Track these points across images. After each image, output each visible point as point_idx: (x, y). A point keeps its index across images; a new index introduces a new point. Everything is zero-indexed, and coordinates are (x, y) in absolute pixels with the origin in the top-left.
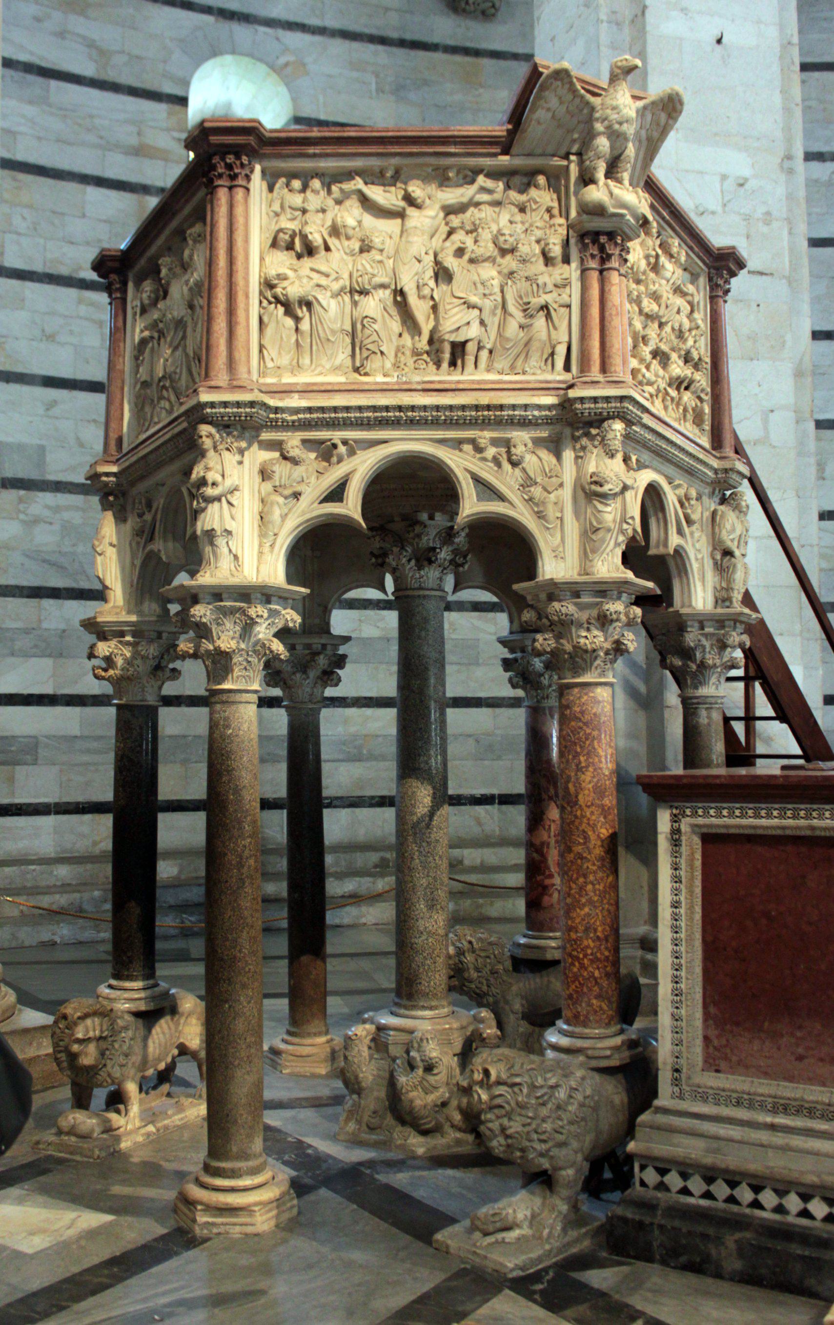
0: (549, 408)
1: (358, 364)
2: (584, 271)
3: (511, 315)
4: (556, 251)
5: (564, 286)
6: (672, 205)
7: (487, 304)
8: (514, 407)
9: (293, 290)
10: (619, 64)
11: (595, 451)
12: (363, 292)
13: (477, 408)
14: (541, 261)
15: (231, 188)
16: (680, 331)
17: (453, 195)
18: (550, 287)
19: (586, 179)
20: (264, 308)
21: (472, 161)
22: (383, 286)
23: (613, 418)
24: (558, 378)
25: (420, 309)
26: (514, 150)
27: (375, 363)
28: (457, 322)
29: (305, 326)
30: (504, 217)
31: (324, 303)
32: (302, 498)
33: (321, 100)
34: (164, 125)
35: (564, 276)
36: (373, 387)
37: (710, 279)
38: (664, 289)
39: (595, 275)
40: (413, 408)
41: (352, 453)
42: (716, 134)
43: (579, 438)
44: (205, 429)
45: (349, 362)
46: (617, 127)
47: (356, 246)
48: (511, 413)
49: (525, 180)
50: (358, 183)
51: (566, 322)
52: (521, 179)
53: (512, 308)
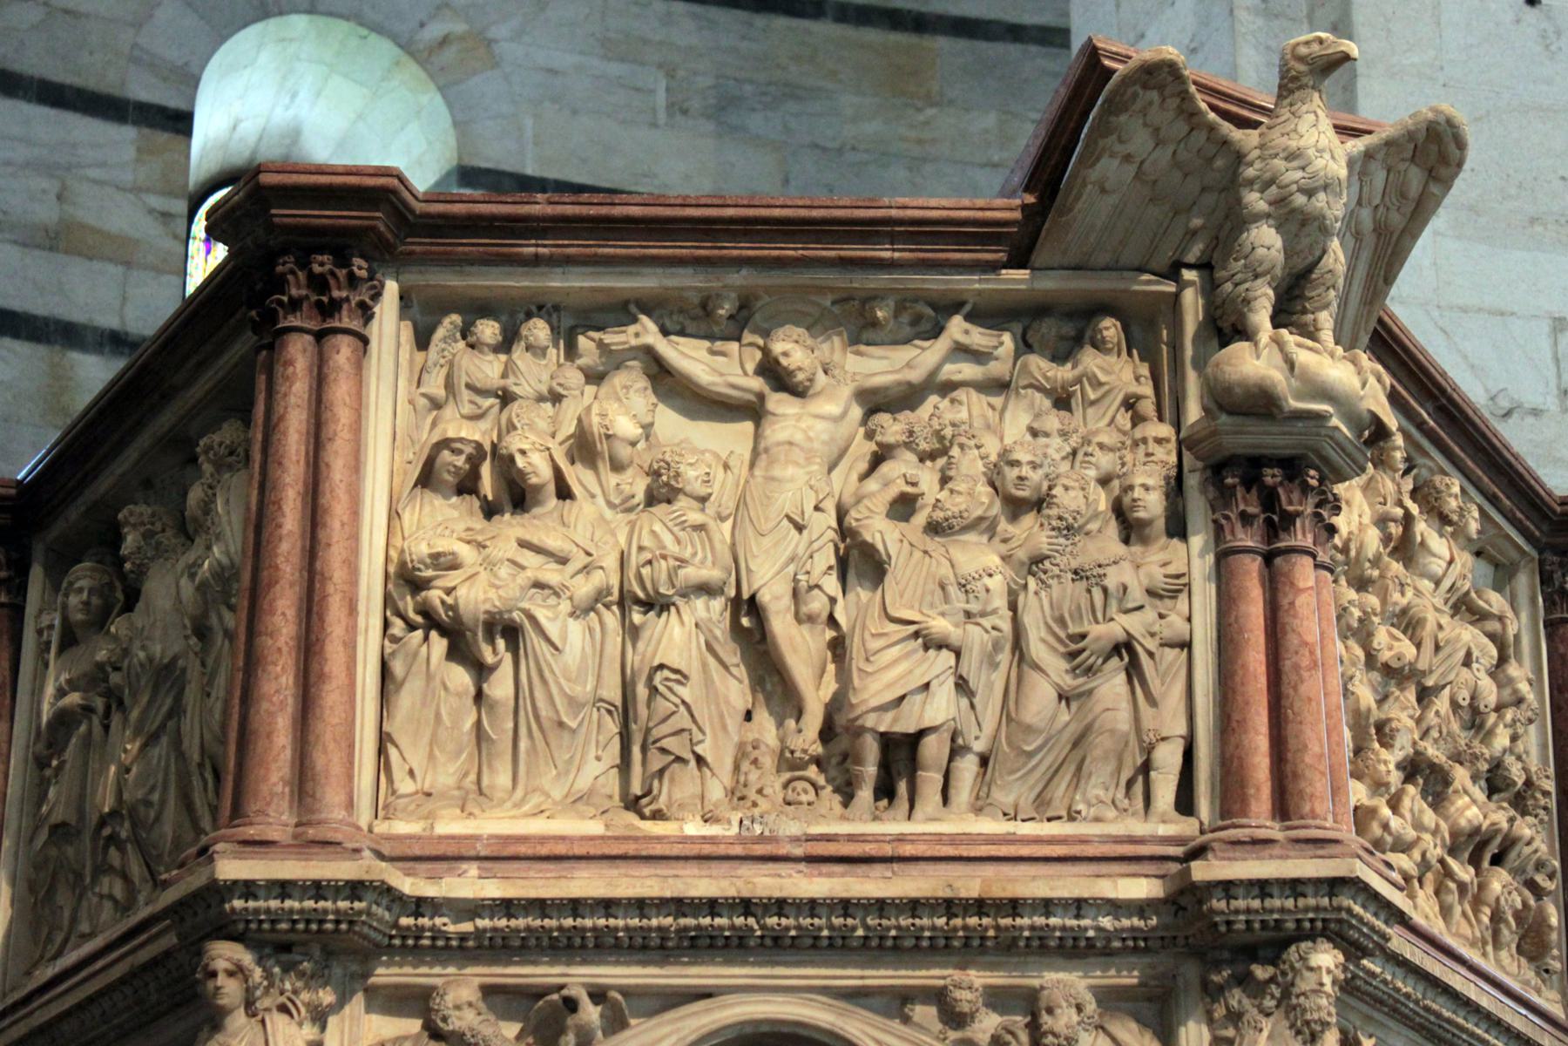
0: (1141, 908)
1: (636, 788)
2: (1224, 556)
3: (1036, 667)
4: (1152, 504)
5: (1174, 594)
6: (1443, 391)
7: (976, 638)
8: (1047, 906)
9: (474, 594)
10: (1303, 50)
11: (1267, 1025)
12: (656, 604)
13: (949, 906)
14: (1113, 529)
15: (320, 336)
16: (1474, 710)
17: (886, 365)
18: (1137, 596)
19: (1227, 327)
20: (395, 640)
21: (935, 282)
22: (706, 589)
23: (1312, 936)
24: (1163, 830)
25: (800, 649)
26: (1039, 258)
27: (681, 787)
28: (897, 683)
29: (501, 687)
30: (1017, 421)
31: (553, 630)
33: (529, 123)
34: (127, 177)
35: (1171, 570)
36: (676, 850)
37: (1546, 579)
38: (1430, 604)
39: (1252, 567)
40: (780, 906)
41: (616, 1023)
42: (1533, 221)
43: (1221, 989)
44: (225, 954)
45: (612, 783)
46: (1300, 200)
47: (639, 486)
48: (1039, 920)
49: (1068, 329)
50: (647, 332)
51: (1179, 687)
52: (1057, 326)
53: (1039, 647)
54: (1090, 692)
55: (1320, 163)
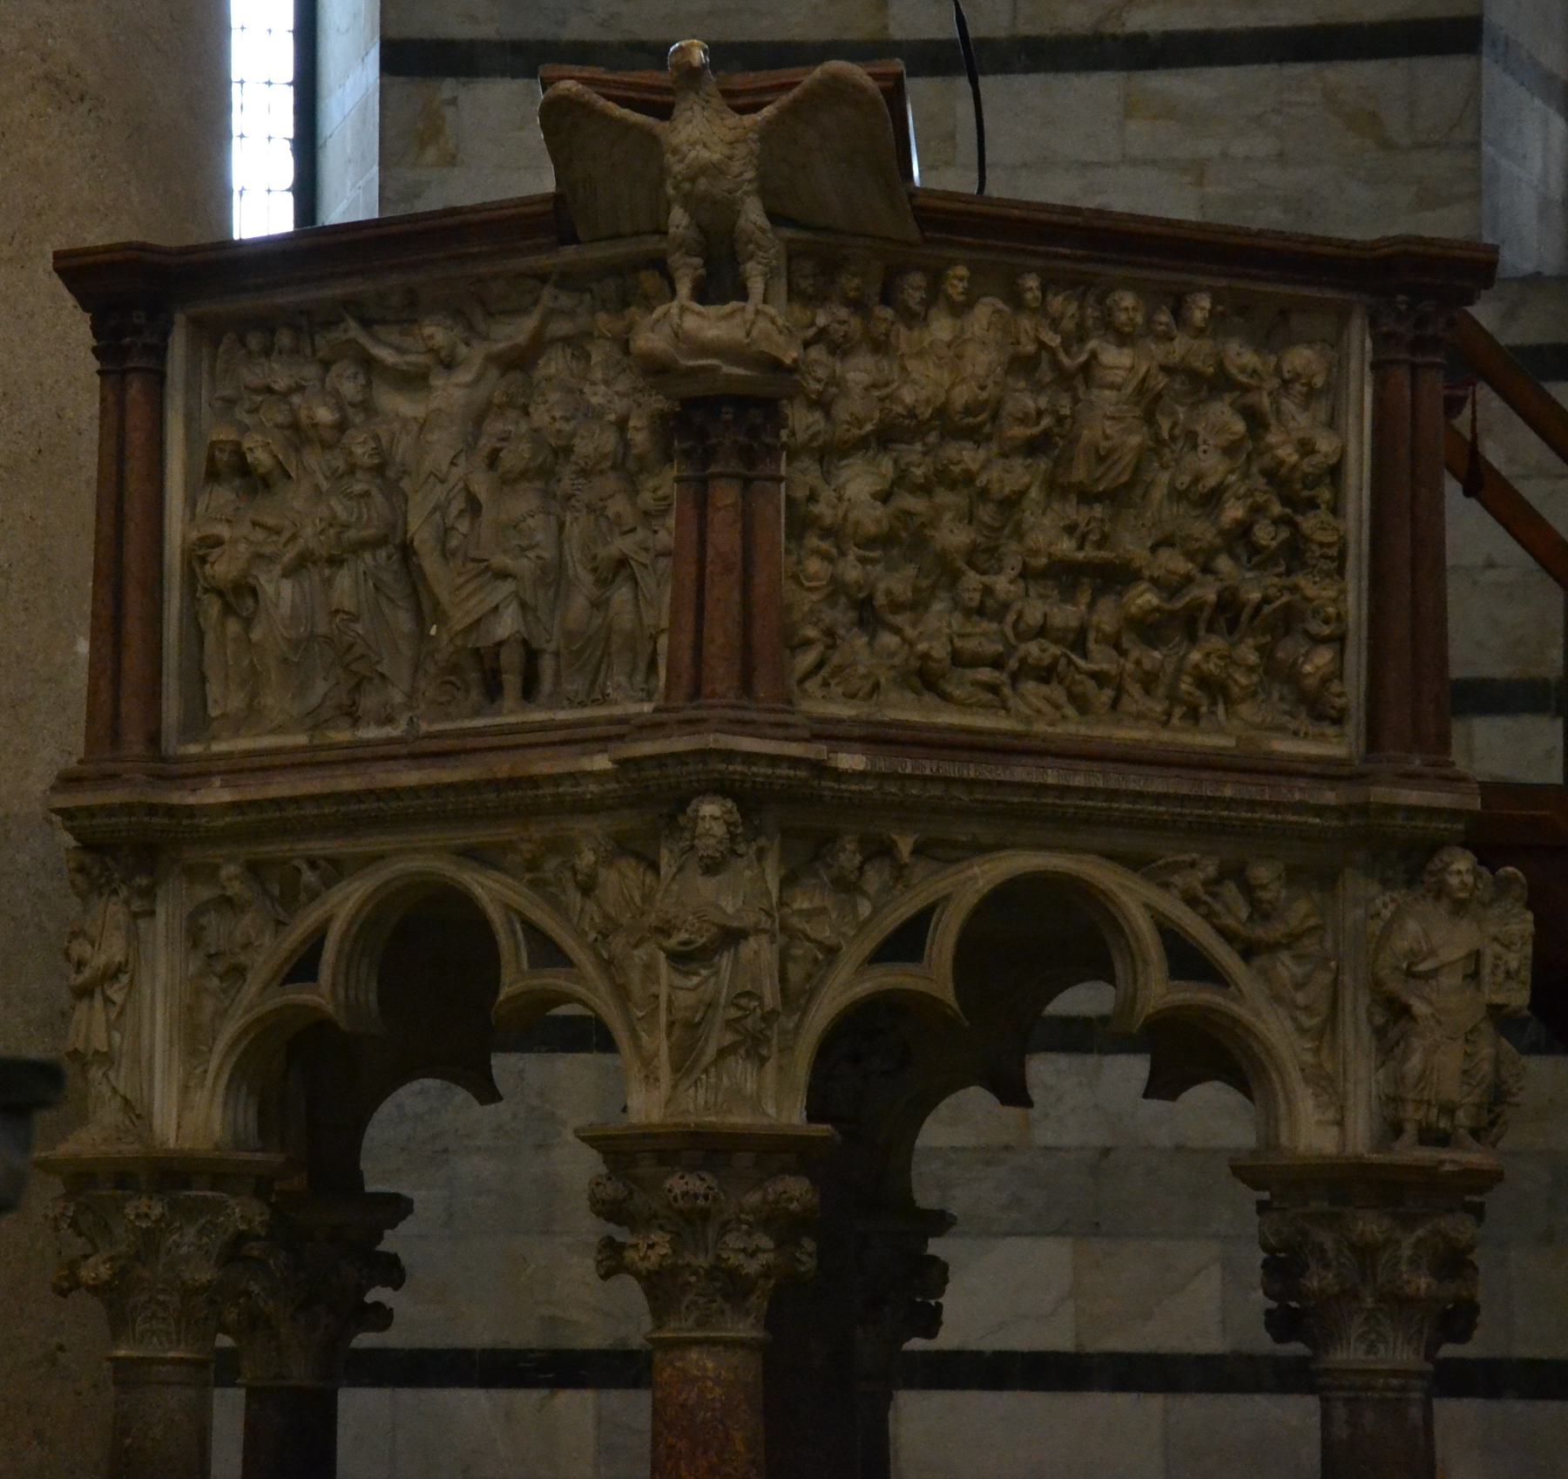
7: (524, 566)
8: (555, 779)
18: (630, 521)
32: (249, 976)
37: (1373, 323)
41: (328, 883)
46: (687, 186)
50: (353, 330)
54: (608, 599)
55: (693, 154)
